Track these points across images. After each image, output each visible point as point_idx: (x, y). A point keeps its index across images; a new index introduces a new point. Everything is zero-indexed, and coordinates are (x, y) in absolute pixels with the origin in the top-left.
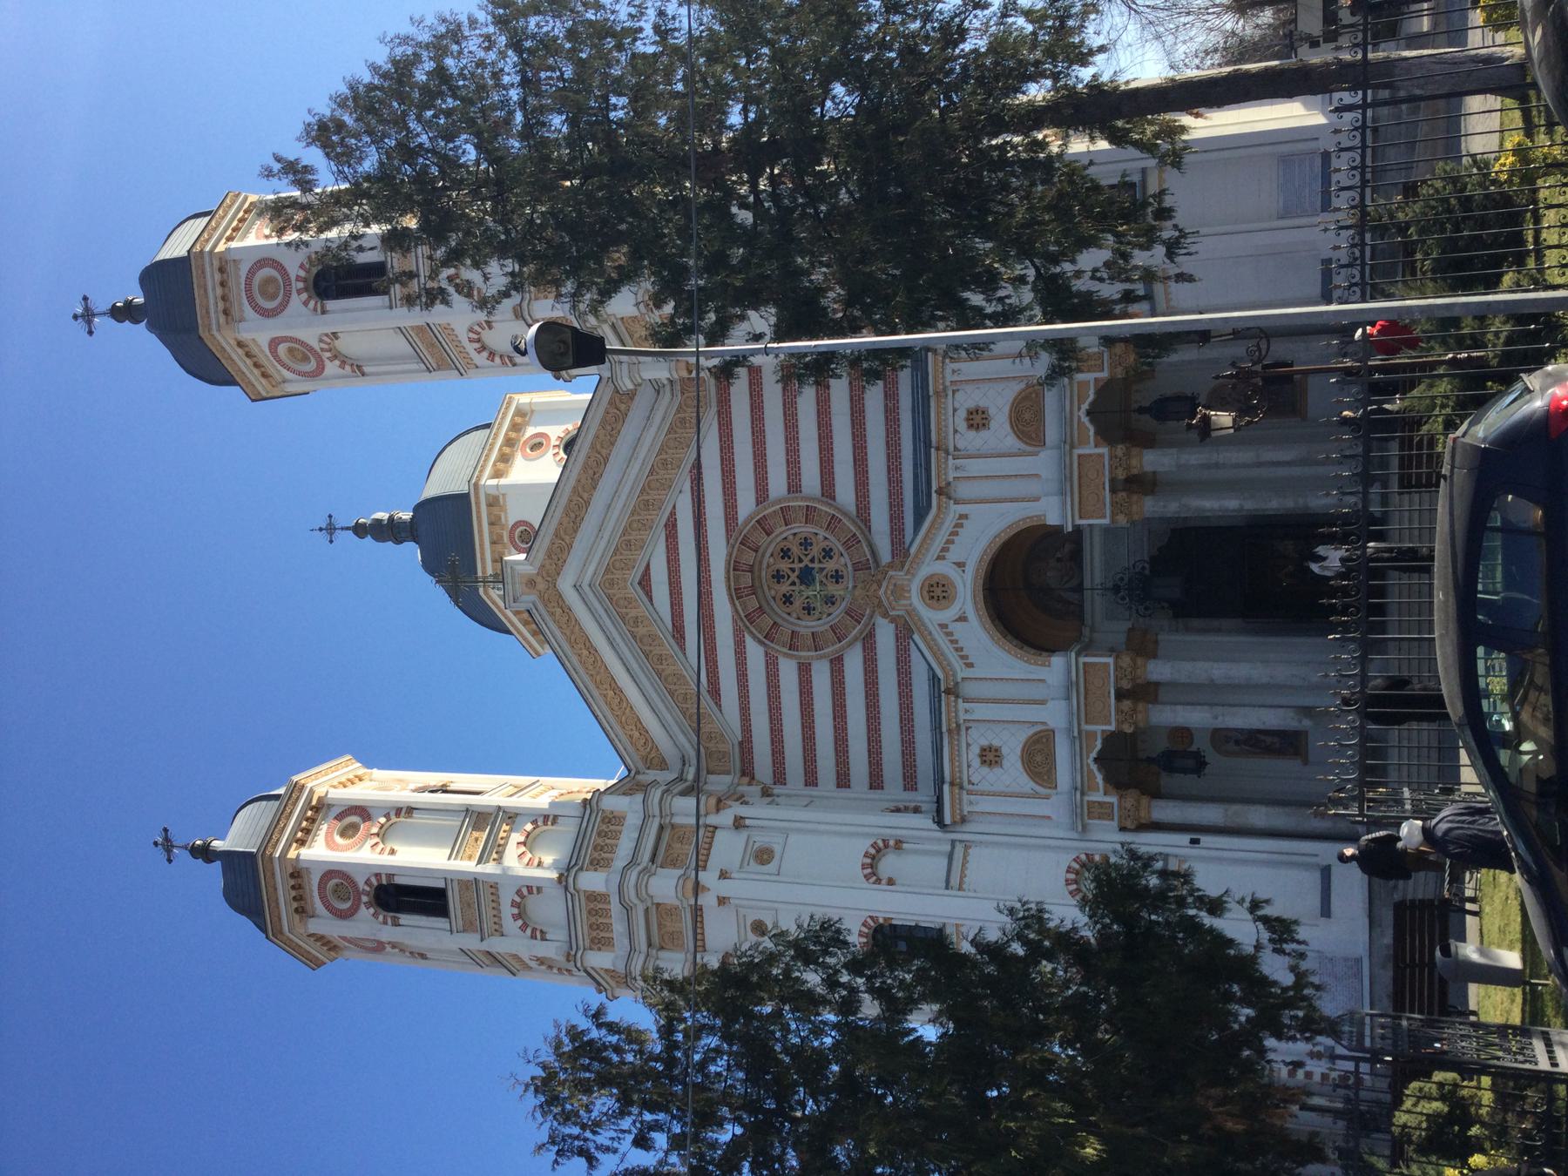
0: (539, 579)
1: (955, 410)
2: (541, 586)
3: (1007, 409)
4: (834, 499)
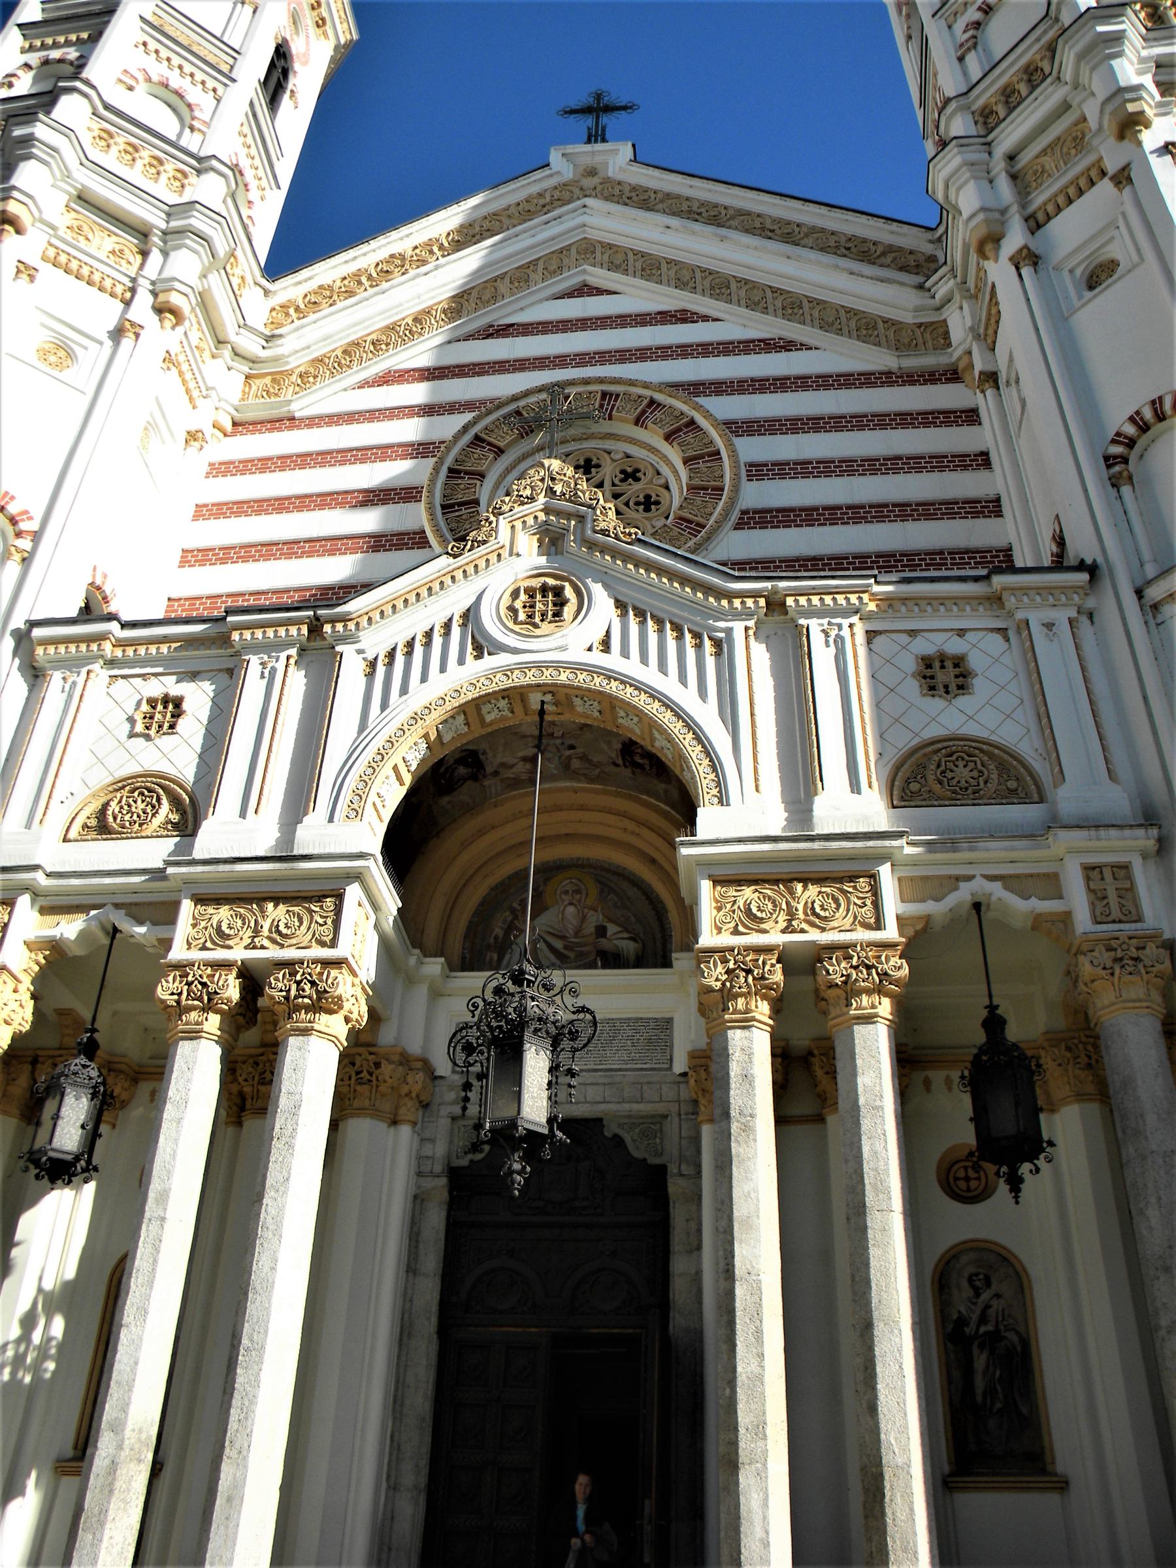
0: (596, 180)
1: (961, 632)
2: (588, 182)
3: (972, 730)
4: (738, 526)
